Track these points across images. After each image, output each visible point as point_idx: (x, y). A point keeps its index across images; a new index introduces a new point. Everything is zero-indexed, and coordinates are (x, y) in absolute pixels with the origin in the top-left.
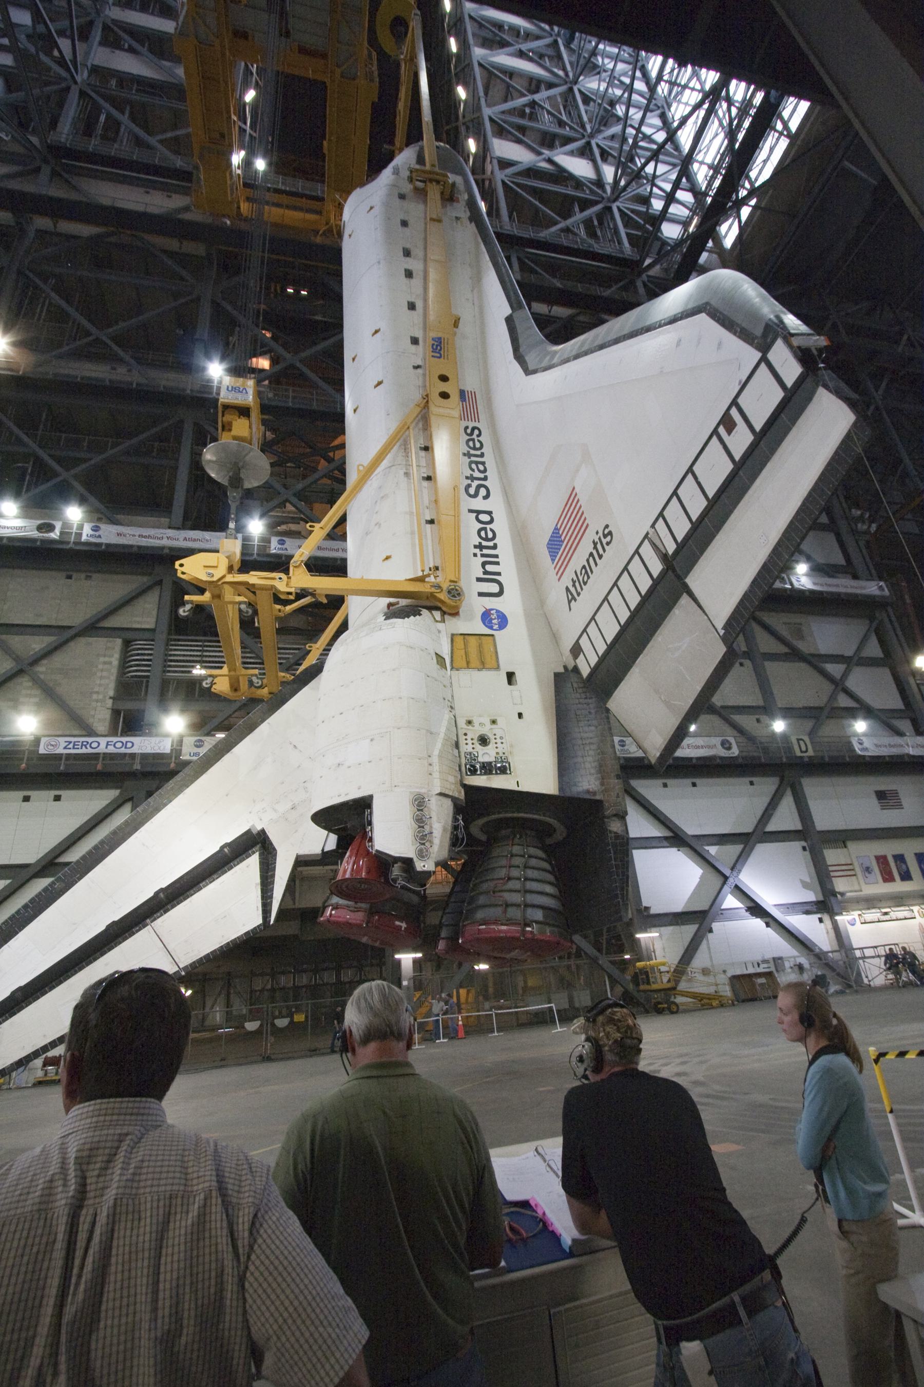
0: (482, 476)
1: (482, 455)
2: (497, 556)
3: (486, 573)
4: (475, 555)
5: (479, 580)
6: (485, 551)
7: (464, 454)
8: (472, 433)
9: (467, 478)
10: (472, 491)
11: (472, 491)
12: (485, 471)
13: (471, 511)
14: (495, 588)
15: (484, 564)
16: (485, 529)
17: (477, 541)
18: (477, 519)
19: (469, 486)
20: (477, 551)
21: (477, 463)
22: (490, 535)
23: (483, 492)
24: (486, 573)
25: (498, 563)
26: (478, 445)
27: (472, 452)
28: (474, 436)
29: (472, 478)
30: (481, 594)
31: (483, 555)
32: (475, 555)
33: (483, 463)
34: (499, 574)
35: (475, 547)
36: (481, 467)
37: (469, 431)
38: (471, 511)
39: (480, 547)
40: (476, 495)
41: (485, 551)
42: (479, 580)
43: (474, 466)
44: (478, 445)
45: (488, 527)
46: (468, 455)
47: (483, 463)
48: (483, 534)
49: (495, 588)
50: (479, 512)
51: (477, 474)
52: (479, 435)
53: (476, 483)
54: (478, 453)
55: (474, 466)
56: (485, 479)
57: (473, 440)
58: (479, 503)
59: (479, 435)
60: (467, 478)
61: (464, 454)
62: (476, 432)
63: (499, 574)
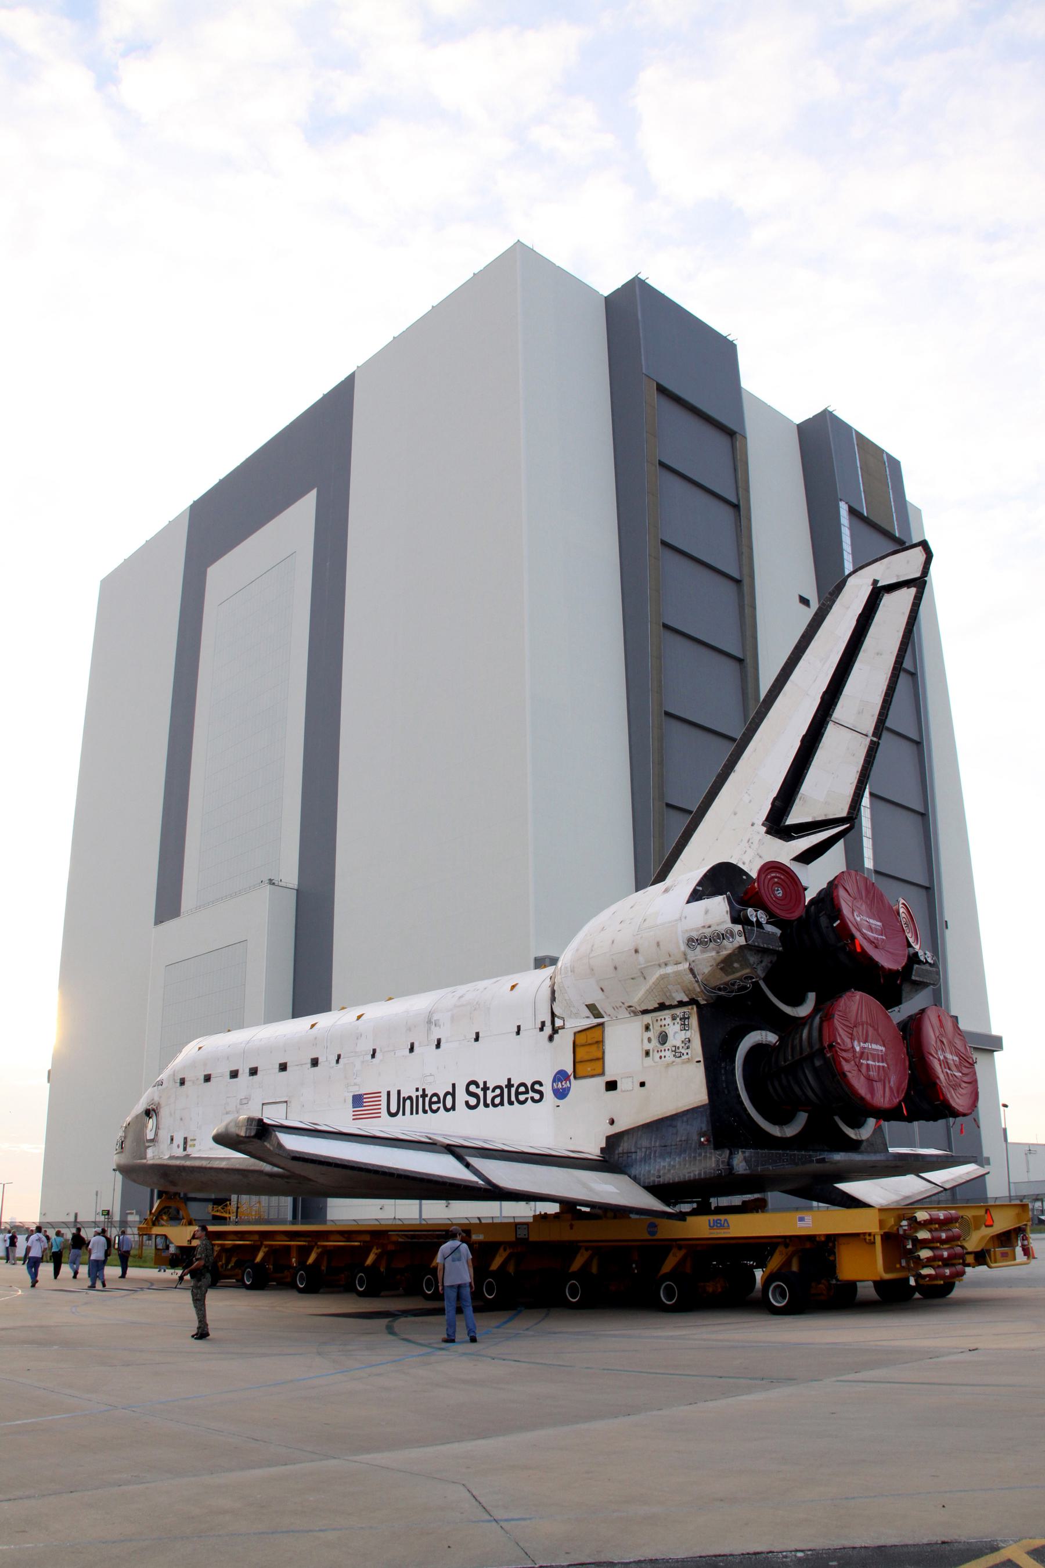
0: (489, 1101)
1: (511, 1103)
2: (417, 1113)
3: (405, 1100)
4: (417, 1090)
5: (399, 1092)
6: (421, 1100)
7: (509, 1080)
8: (534, 1091)
9: (485, 1083)
10: (473, 1088)
11: (473, 1088)
12: (495, 1105)
13: (454, 1085)
14: (393, 1109)
15: (410, 1098)
16: (438, 1102)
17: (429, 1093)
18: (447, 1093)
19: (478, 1086)
20: (420, 1093)
21: (501, 1095)
22: (434, 1107)
23: (473, 1101)
24: (405, 1100)
25: (412, 1113)
26: (522, 1098)
27: (513, 1090)
28: (531, 1094)
29: (485, 1089)
30: (389, 1093)
31: (417, 1097)
32: (417, 1090)
33: (502, 1103)
34: (404, 1114)
35: (424, 1090)
36: (497, 1101)
37: (537, 1087)
38: (454, 1085)
39: (424, 1096)
40: (470, 1093)
41: (421, 1100)
42: (399, 1092)
43: (498, 1091)
44: (522, 1098)
45: (441, 1105)
46: (509, 1085)
47: (502, 1103)
48: (435, 1099)
49: (393, 1109)
50: (453, 1095)
51: (490, 1095)
52: (532, 1099)
53: (481, 1094)
54: (513, 1098)
55: (498, 1091)
56: (486, 1105)
57: (527, 1092)
58: (461, 1096)
59: (533, 1100)
60: (485, 1083)
61: (509, 1080)
62: (537, 1096)
63: (404, 1114)
